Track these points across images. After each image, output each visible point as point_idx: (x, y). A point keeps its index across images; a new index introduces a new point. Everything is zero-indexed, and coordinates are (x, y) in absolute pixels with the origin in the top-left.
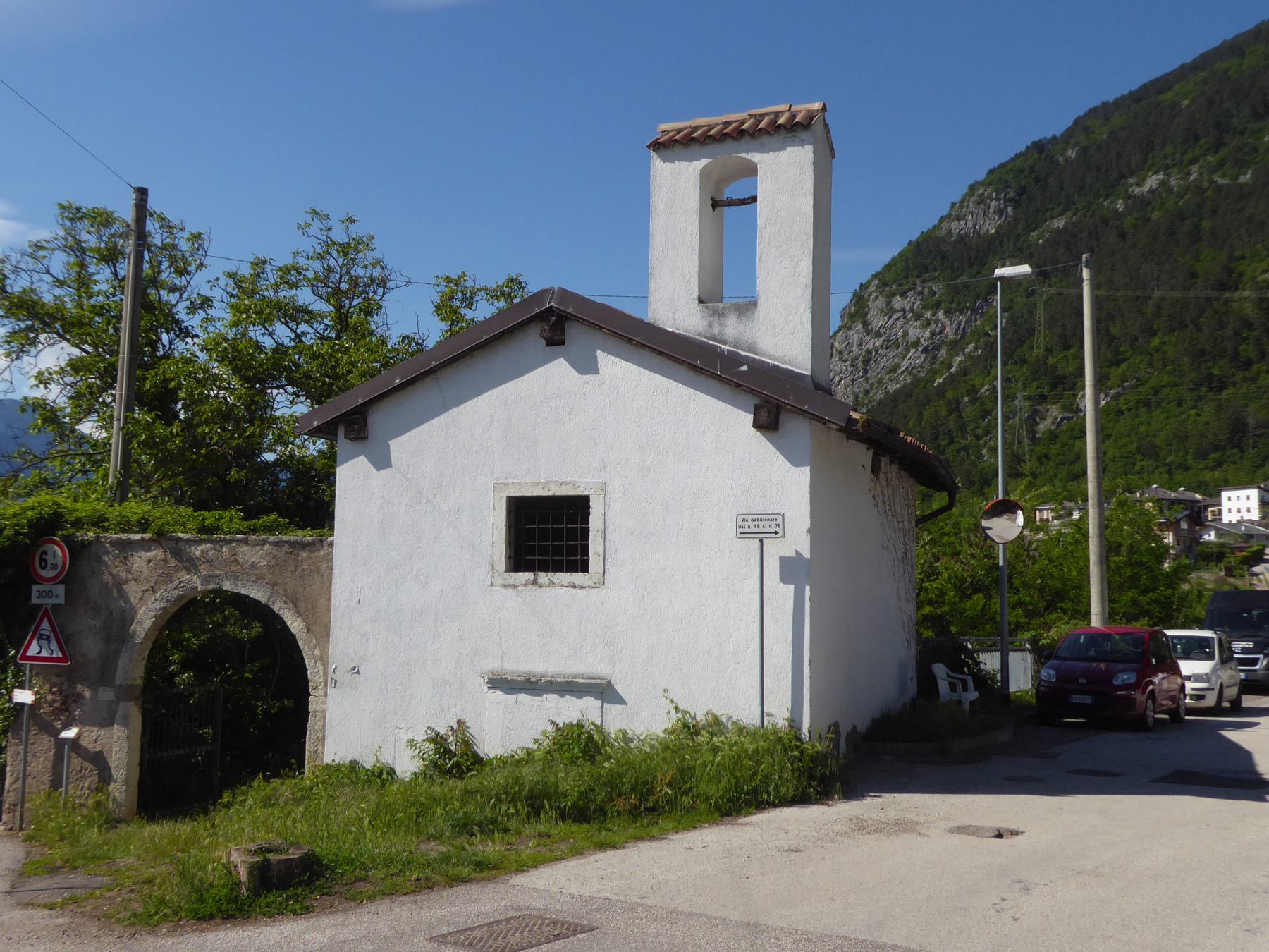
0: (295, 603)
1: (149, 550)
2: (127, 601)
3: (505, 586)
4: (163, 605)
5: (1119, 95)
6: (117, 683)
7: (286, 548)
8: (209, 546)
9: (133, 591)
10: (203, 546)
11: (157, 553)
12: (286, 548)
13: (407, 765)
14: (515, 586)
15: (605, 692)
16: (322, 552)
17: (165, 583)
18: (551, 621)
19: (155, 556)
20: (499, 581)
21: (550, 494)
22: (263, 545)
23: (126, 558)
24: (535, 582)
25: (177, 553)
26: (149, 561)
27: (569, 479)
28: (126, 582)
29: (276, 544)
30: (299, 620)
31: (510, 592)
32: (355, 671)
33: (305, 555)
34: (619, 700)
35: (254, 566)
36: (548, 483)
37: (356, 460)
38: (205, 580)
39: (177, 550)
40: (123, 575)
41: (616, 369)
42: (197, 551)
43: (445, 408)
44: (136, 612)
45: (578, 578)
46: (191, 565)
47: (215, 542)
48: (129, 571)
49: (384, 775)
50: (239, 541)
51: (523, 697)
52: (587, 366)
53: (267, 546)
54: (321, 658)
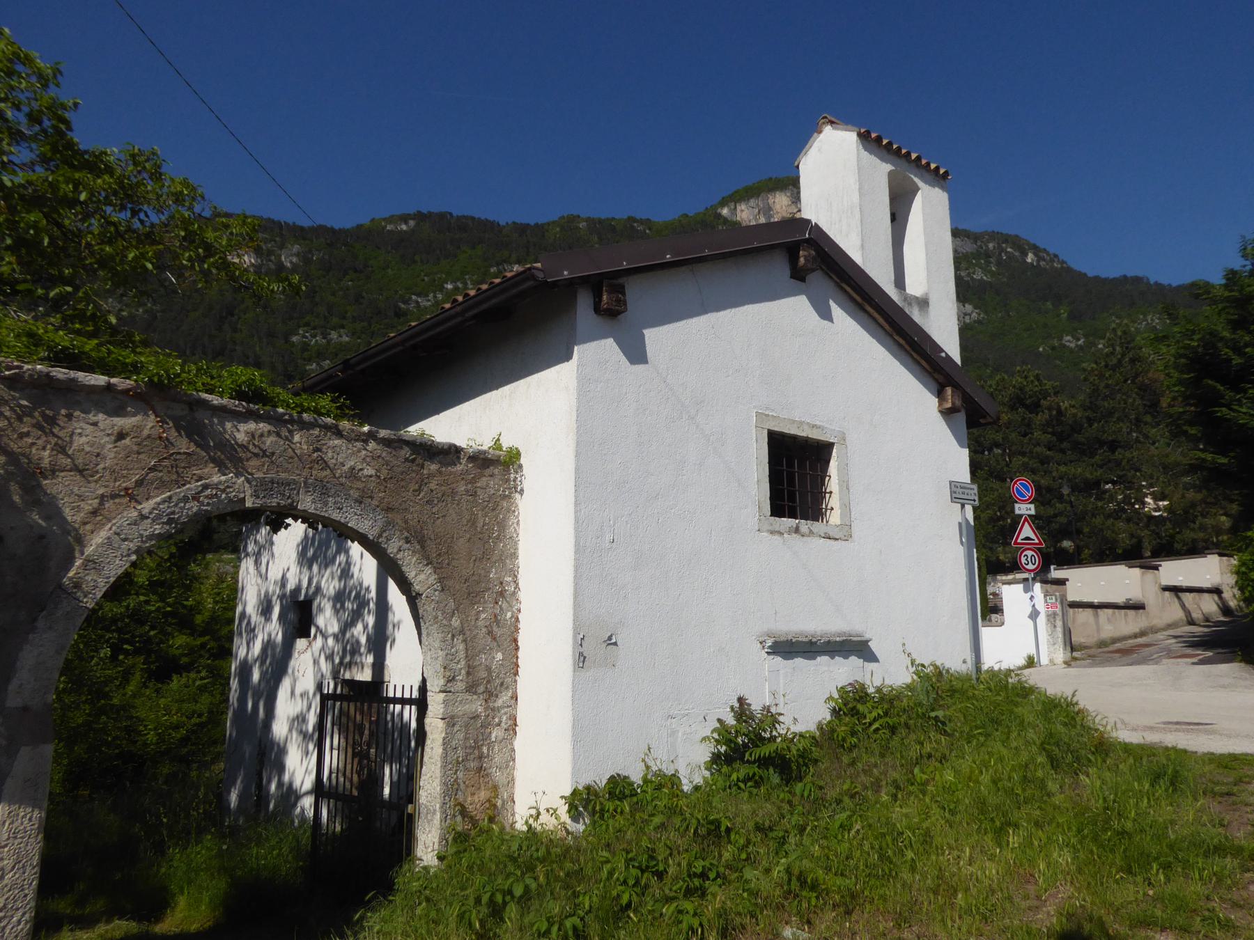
0: (422, 542)
1: (119, 411)
2: (52, 511)
3: (772, 533)
4: (158, 529)
5: (491, 218)
6: (13, 701)
7: (406, 452)
8: (263, 427)
9: (71, 497)
10: (252, 426)
11: (147, 423)
12: (406, 452)
13: (690, 759)
14: (781, 534)
15: (857, 648)
16: (459, 468)
17: (163, 485)
18: (802, 577)
19: (139, 428)
20: (766, 527)
21: (804, 434)
22: (366, 442)
23: (52, 421)
24: (797, 530)
25: (195, 431)
26: (121, 436)
27: (818, 423)
28: (53, 471)
29: (387, 442)
30: (429, 570)
31: (776, 537)
32: (610, 642)
33: (434, 467)
34: (870, 657)
35: (353, 474)
36: (801, 423)
37: (603, 342)
38: (263, 487)
39: (192, 419)
40: (46, 457)
41: (846, 327)
42: (242, 432)
43: (703, 309)
44: (80, 541)
45: (817, 526)
46: (229, 456)
47: (277, 421)
48: (61, 449)
49: (665, 783)
50: (326, 427)
51: (799, 661)
52: (826, 315)
53: (372, 445)
54: (462, 632)
